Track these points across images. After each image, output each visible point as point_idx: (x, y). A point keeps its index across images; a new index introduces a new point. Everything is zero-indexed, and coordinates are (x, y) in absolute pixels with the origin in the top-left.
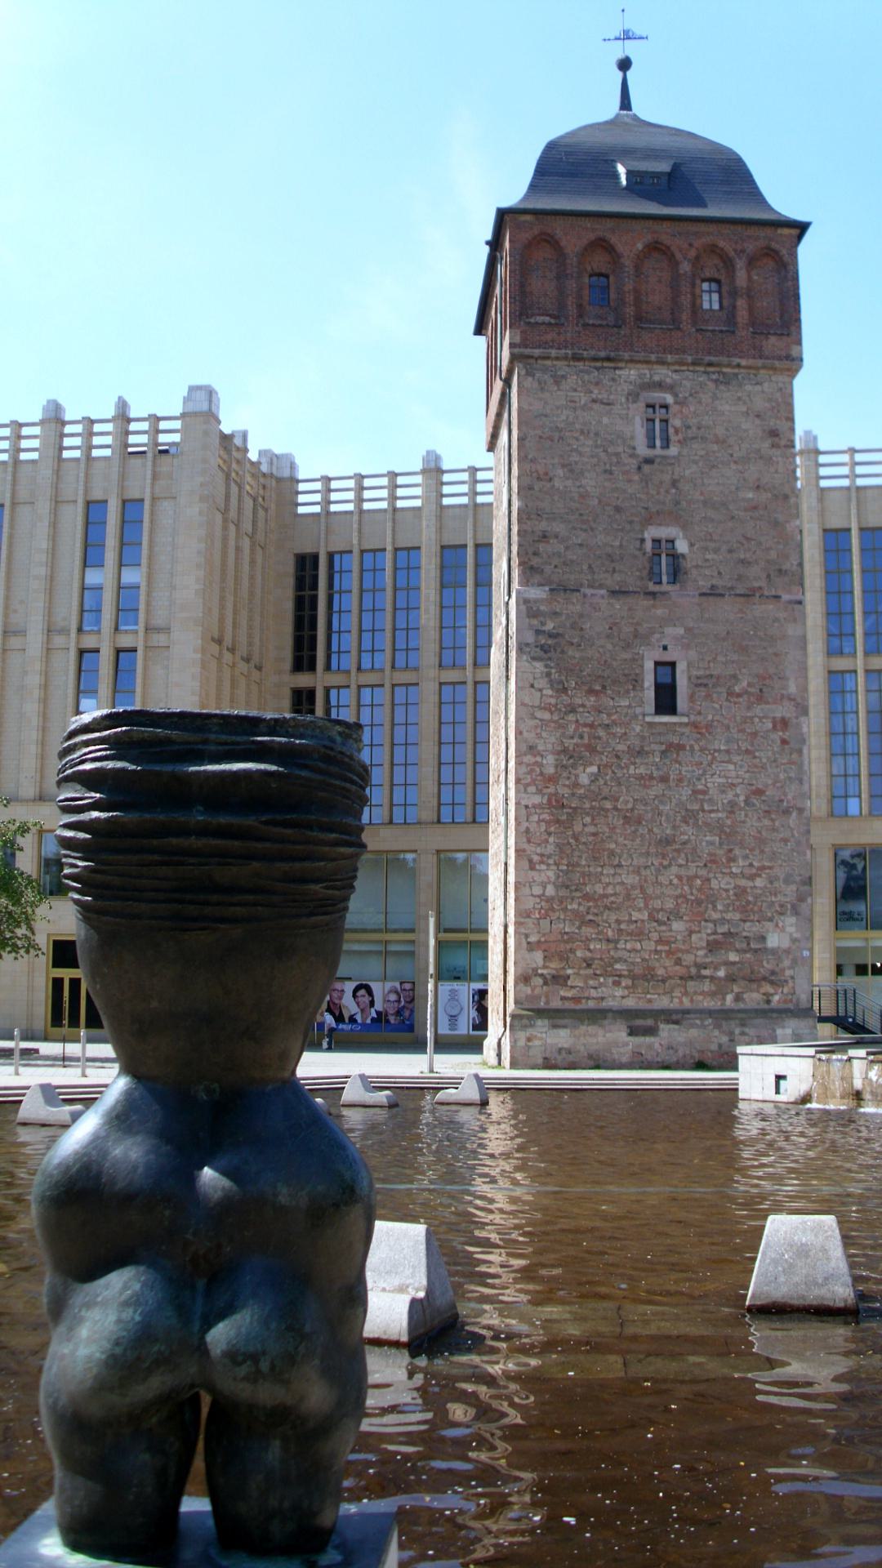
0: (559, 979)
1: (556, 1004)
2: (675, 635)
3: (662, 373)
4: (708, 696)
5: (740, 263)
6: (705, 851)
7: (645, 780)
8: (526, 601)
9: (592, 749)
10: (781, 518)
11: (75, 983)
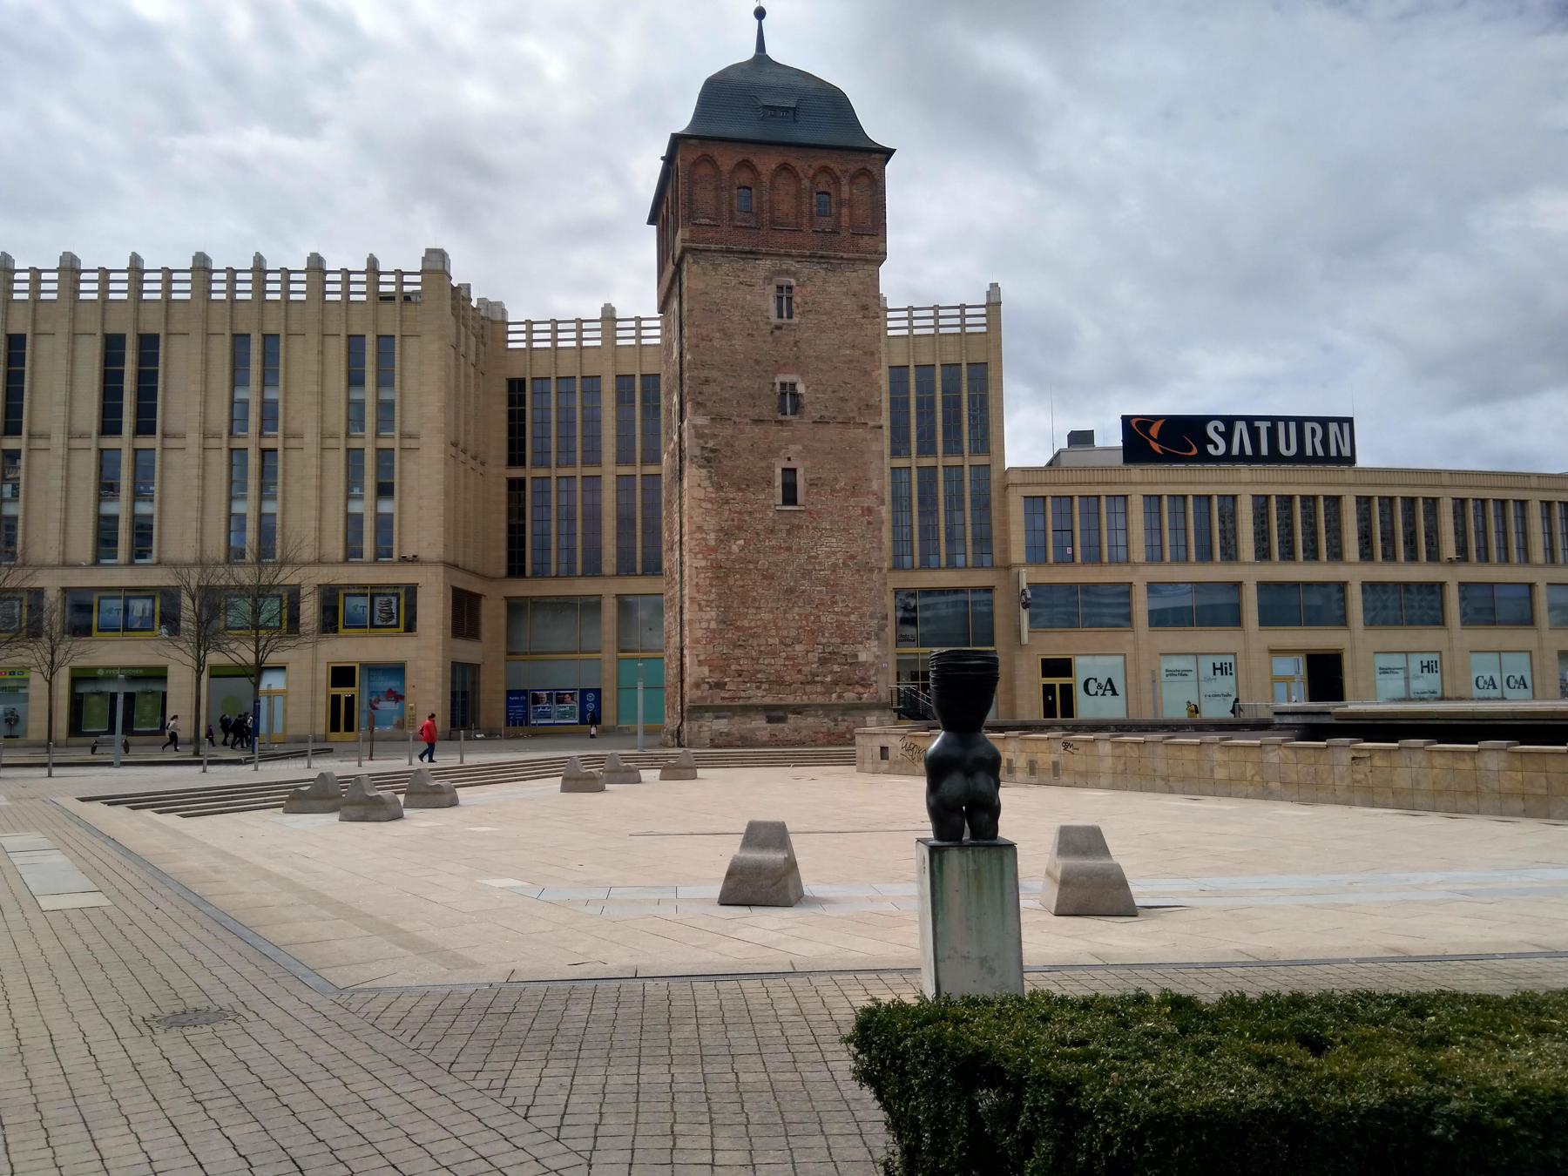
0: (719, 685)
1: (718, 702)
2: (795, 449)
3: (789, 264)
5: (844, 181)
6: (816, 596)
7: (776, 549)
8: (695, 426)
9: (740, 528)
10: (869, 368)
11: (350, 701)
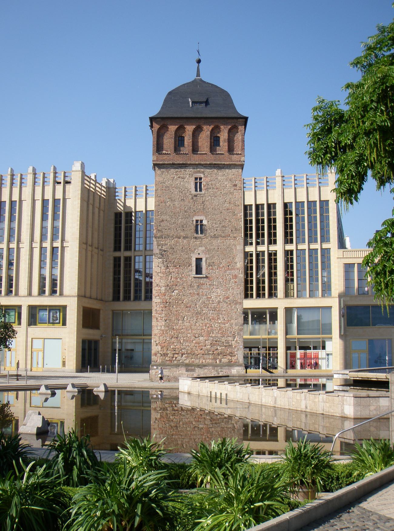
4: (212, 269)
